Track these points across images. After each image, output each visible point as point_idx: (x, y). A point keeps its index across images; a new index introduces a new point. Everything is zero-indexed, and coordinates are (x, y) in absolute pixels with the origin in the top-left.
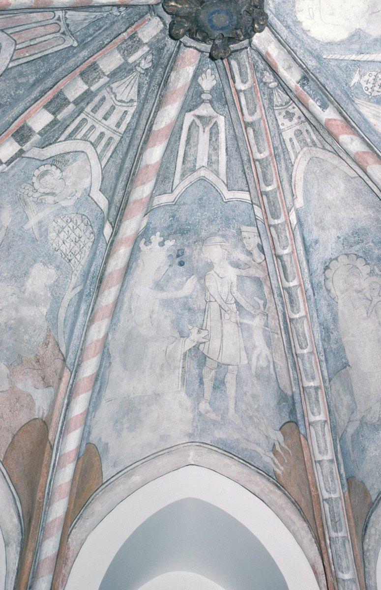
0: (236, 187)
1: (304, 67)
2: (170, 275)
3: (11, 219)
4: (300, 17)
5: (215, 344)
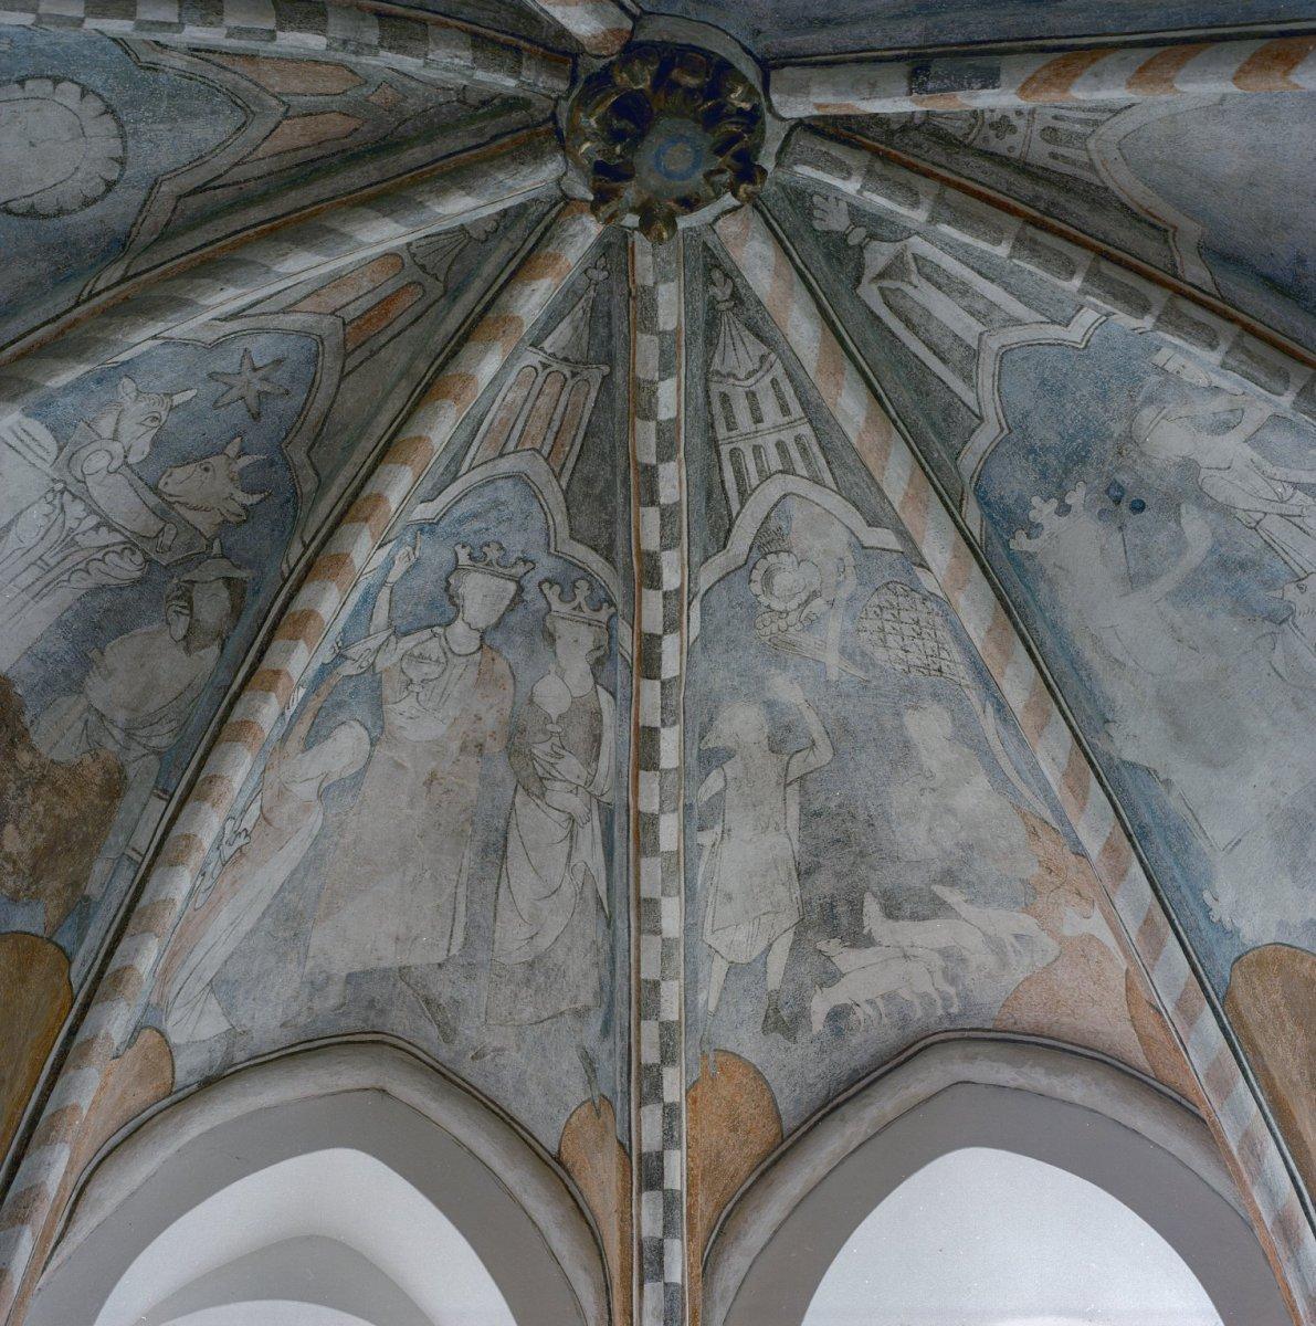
0: (1070, 311)
1: (906, 52)
2: (1138, 542)
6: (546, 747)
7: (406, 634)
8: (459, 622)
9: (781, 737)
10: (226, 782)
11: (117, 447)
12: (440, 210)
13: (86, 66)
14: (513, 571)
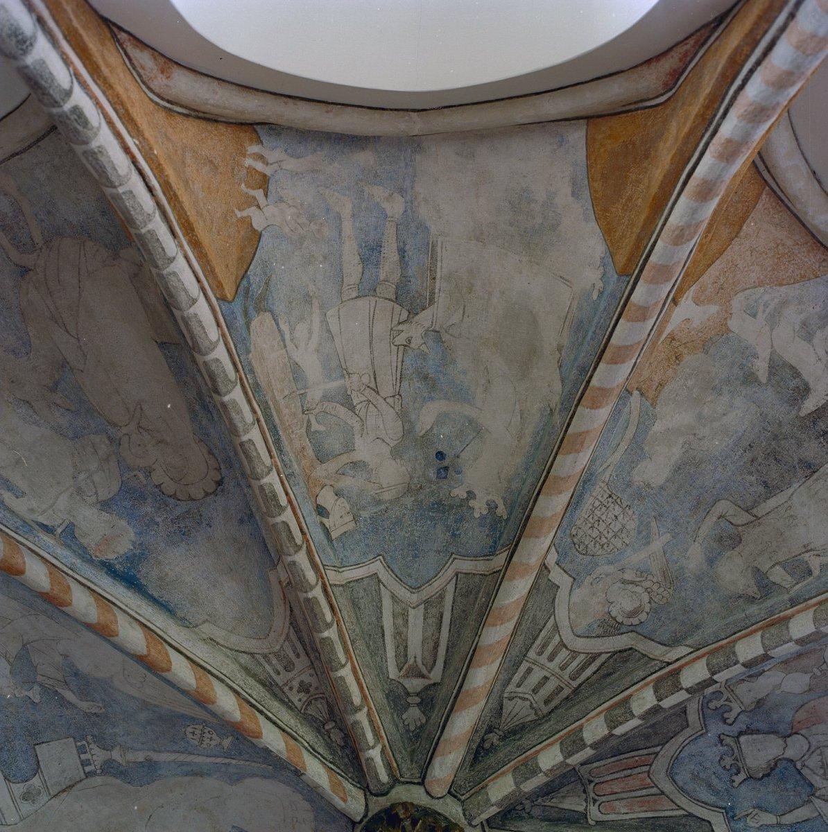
2: (458, 442)
3: (688, 553)
4: (307, 805)
5: (381, 327)
7: (811, 785)
8: (785, 756)
9: (729, 540)
14: (732, 743)
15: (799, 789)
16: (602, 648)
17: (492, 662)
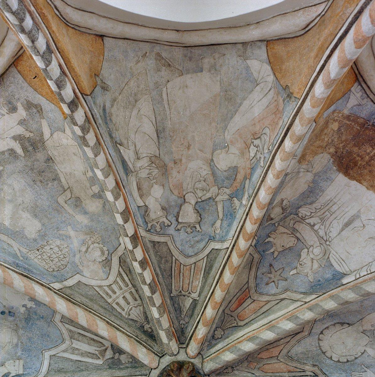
0: (52, 362)
6: (154, 174)
7: (210, 198)
8: (194, 204)
9: (77, 202)
10: (267, 194)
11: (312, 256)
12: (234, 356)
13: (332, 366)
14: (181, 226)
15: (210, 204)
16: (116, 269)
17: (97, 326)
